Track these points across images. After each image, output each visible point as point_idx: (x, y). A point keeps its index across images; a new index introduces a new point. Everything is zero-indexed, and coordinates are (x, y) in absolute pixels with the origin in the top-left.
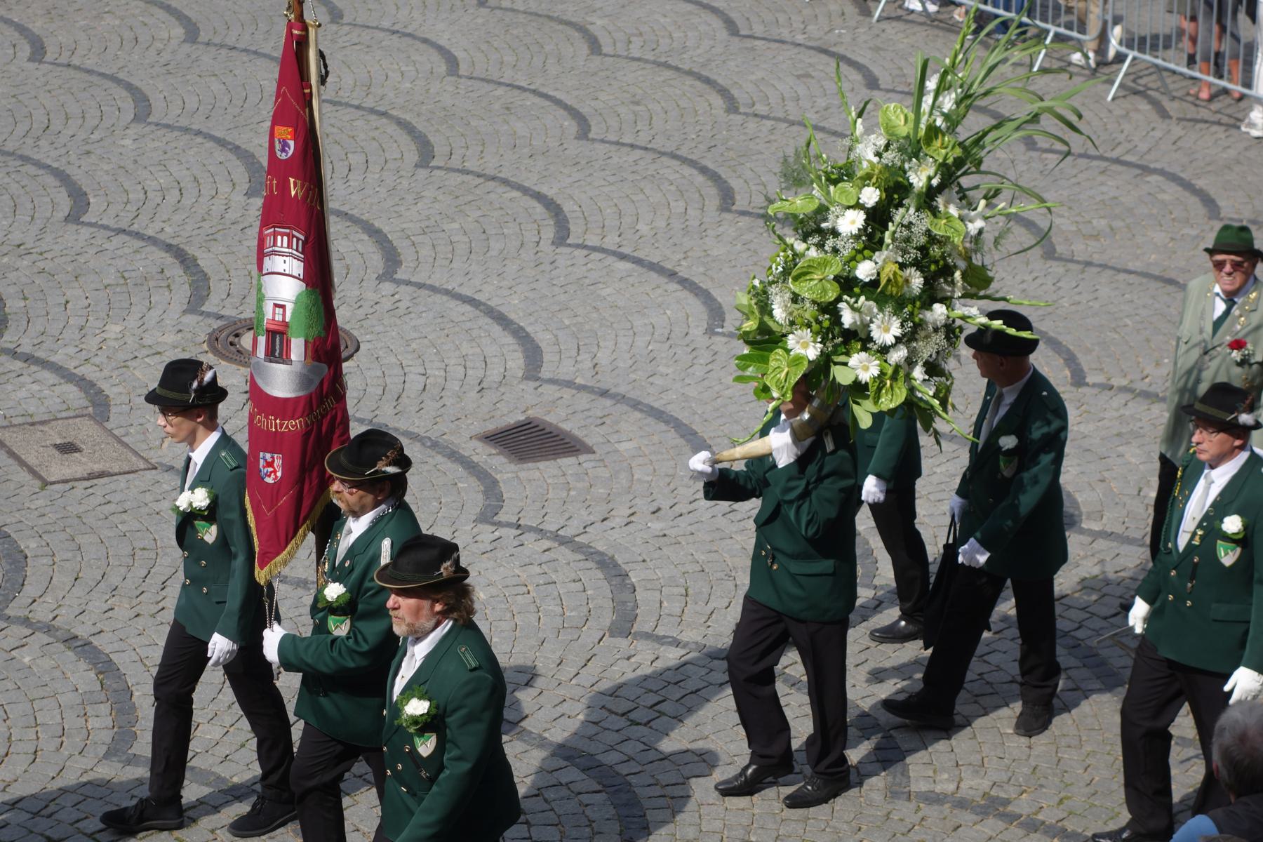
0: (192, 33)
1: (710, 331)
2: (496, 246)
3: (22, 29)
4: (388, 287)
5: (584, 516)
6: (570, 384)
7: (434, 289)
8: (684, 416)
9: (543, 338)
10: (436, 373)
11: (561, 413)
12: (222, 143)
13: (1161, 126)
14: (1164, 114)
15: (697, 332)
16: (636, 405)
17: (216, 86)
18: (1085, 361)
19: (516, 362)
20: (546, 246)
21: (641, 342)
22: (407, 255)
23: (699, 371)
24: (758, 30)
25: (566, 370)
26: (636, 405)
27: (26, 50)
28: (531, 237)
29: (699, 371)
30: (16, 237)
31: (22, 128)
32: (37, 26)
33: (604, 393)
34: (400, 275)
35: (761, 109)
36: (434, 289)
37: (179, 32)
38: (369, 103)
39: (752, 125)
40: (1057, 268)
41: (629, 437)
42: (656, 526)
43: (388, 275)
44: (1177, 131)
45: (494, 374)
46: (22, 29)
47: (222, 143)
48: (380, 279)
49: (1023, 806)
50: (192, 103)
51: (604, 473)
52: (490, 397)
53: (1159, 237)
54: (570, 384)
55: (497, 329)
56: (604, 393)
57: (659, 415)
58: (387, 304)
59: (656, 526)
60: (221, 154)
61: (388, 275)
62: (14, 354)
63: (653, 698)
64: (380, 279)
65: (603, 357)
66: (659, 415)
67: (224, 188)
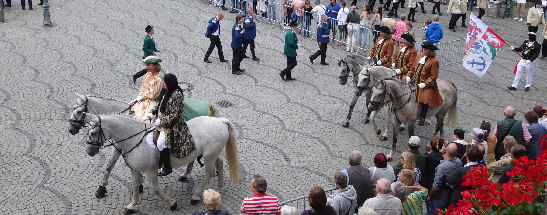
0: (165, 33)
1: (255, 85)
2: (218, 70)
3: (136, 32)
4: (199, 77)
5: (234, 118)
6: (231, 94)
7: (208, 78)
8: (251, 100)
9: (226, 86)
10: (208, 92)
11: (229, 99)
12: (171, 52)
13: (333, 50)
14: (334, 48)
15: (253, 85)
16: (243, 98)
17: (170, 42)
18: (321, 90)
19: (222, 90)
20: (227, 70)
21: (243, 87)
22: (203, 71)
23: (254, 92)
24: (264, 33)
25: (230, 92)
26: (243, 98)
27: (136, 36)
28: (224, 68)
29: (254, 92)
30: (134, 68)
31: (135, 49)
32: (138, 32)
33: (237, 96)
34: (202, 75)
35: (264, 46)
36: (208, 78)
37: (163, 33)
38: (196, 45)
39: (262, 49)
40: (316, 74)
41: (241, 103)
42: (246, 119)
43: (199, 75)
44: (336, 51)
45: (218, 92)
46: (136, 32)
47: (171, 52)
48: (198, 75)
49: (311, 168)
50: (165, 45)
51: (237, 110)
52: (217, 96)
53: (334, 69)
54: (231, 94)
55: (218, 85)
56: (237, 96)
57: (247, 100)
58: (199, 80)
59: (246, 119)
60: (170, 54)
61: (199, 75)
62: (134, 89)
63: (246, 150)
64: (198, 75)
65: (237, 89)
66: (247, 100)
67: (171, 60)
